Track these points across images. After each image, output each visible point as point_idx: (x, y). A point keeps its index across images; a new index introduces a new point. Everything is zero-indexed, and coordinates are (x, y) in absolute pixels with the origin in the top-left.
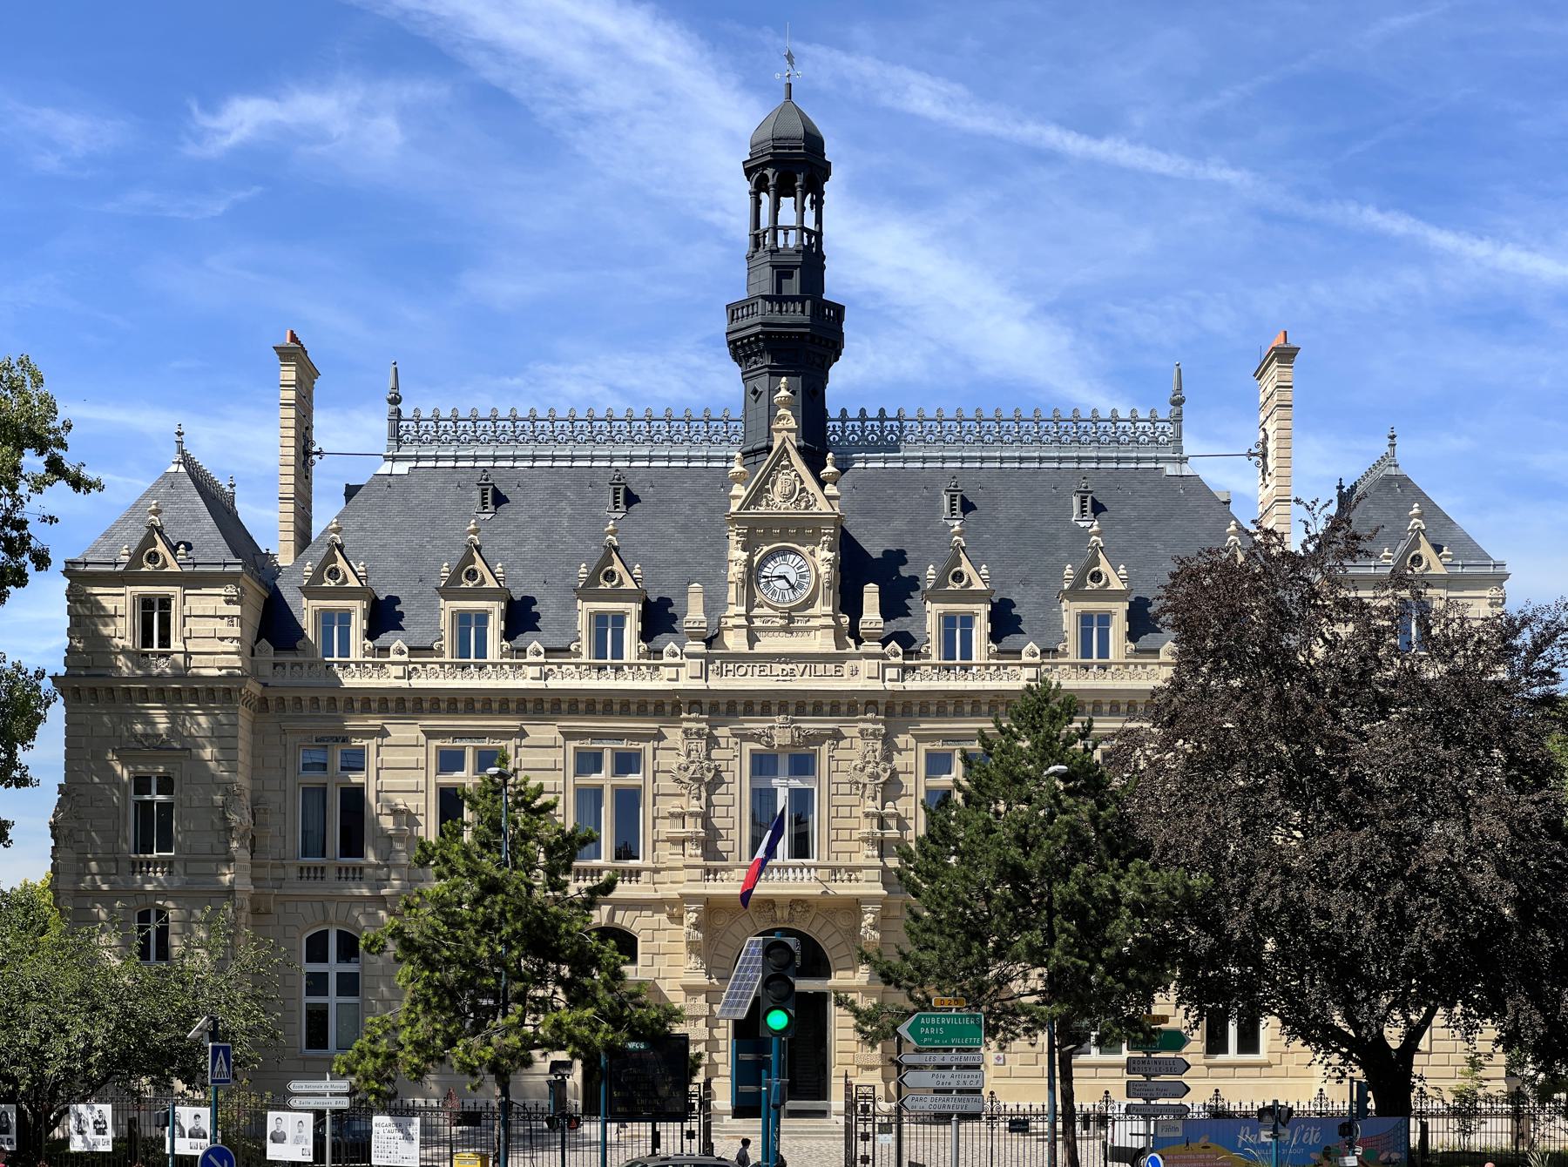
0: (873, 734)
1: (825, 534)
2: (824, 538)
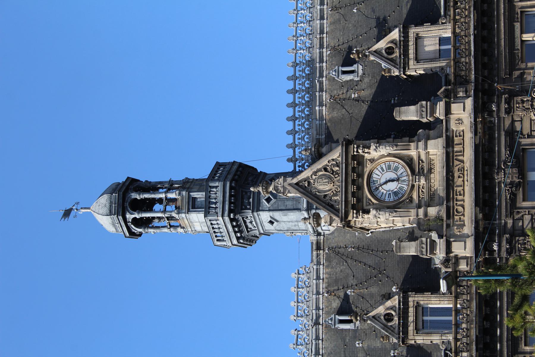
0: (509, 103)
1: (357, 152)
2: (360, 151)
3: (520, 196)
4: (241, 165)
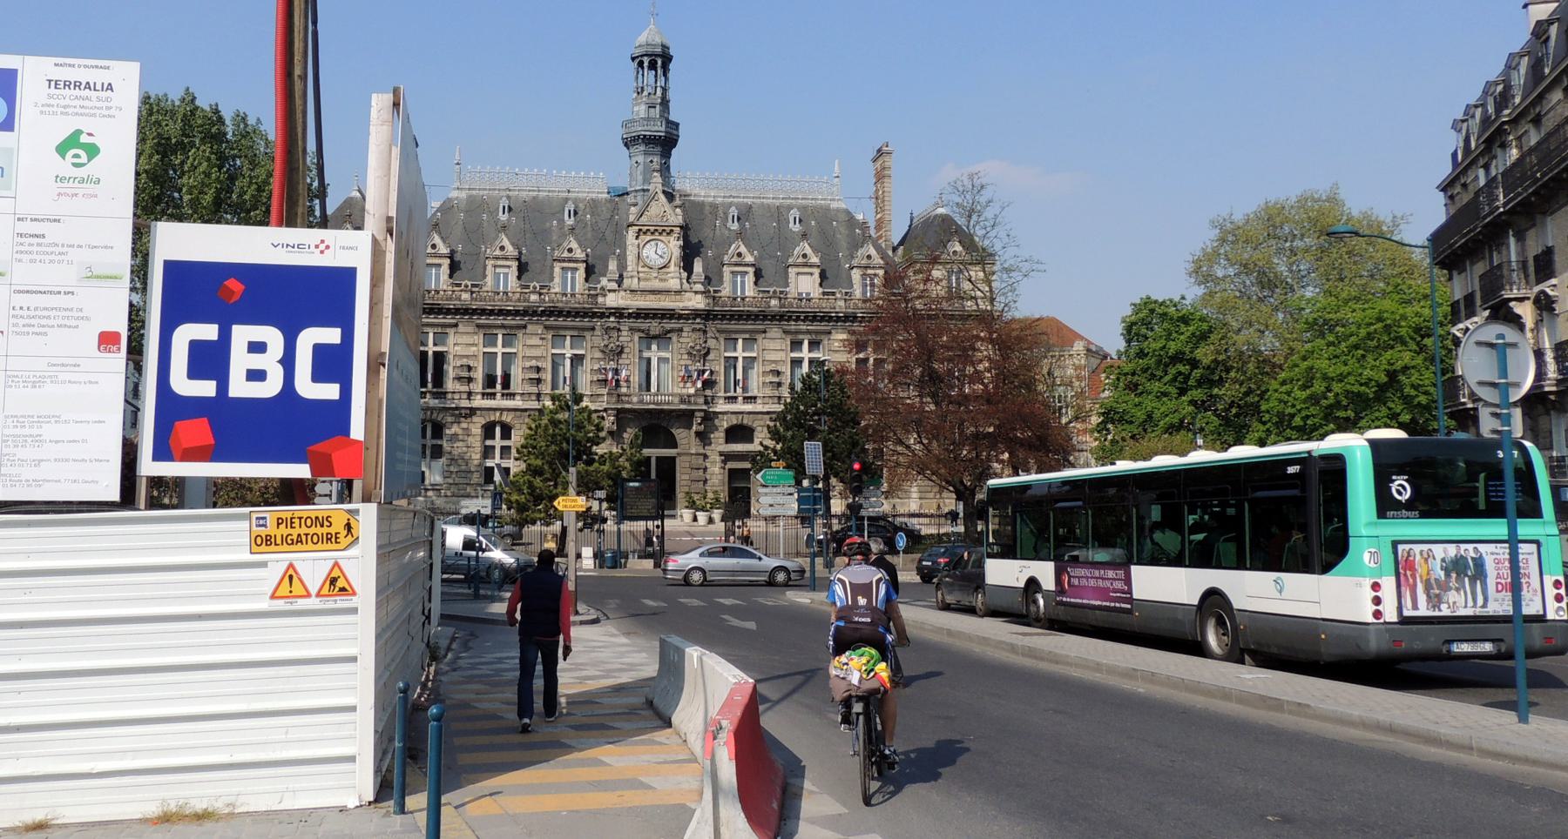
3: (642, 335)
4: (677, 141)
